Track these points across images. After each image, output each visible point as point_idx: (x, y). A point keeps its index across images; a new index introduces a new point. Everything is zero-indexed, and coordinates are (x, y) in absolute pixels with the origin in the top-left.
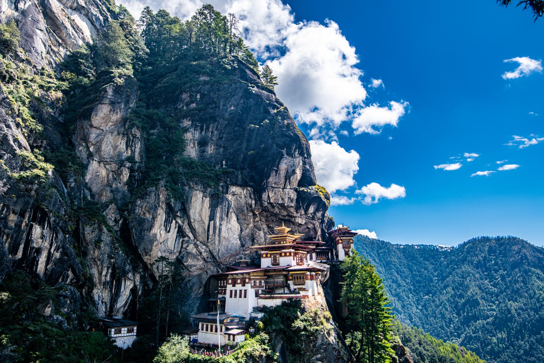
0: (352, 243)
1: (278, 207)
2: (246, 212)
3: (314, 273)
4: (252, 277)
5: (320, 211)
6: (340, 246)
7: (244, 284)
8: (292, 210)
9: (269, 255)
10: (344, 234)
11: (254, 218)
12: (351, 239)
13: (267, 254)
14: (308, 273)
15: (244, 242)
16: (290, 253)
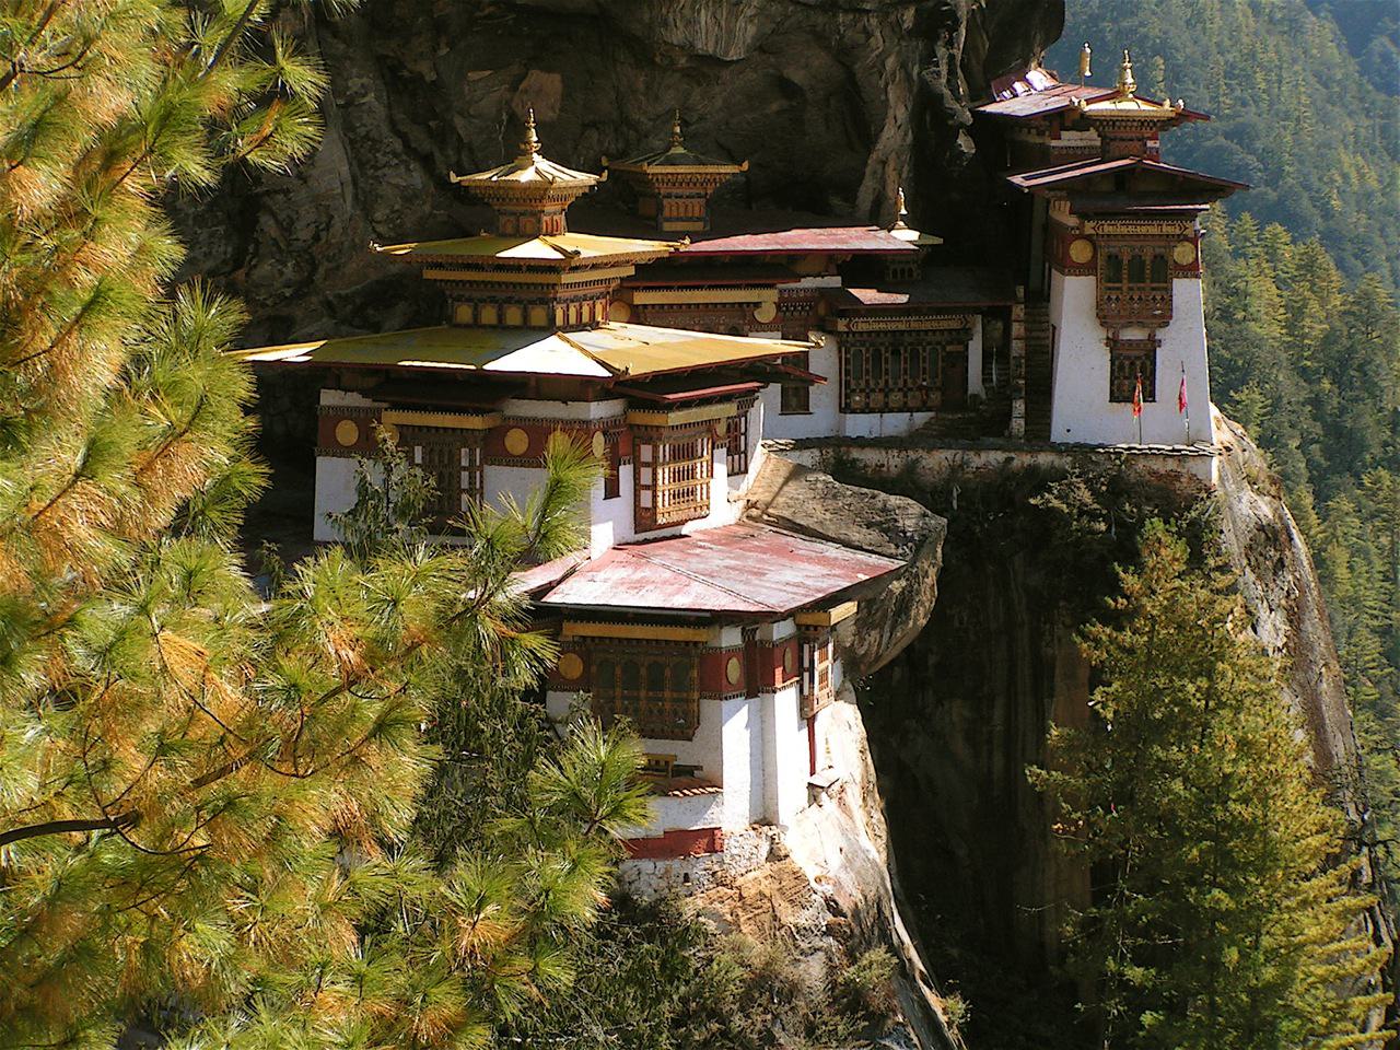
0: (1190, 271)
6: (1074, 296)
9: (386, 435)
14: (731, 638)
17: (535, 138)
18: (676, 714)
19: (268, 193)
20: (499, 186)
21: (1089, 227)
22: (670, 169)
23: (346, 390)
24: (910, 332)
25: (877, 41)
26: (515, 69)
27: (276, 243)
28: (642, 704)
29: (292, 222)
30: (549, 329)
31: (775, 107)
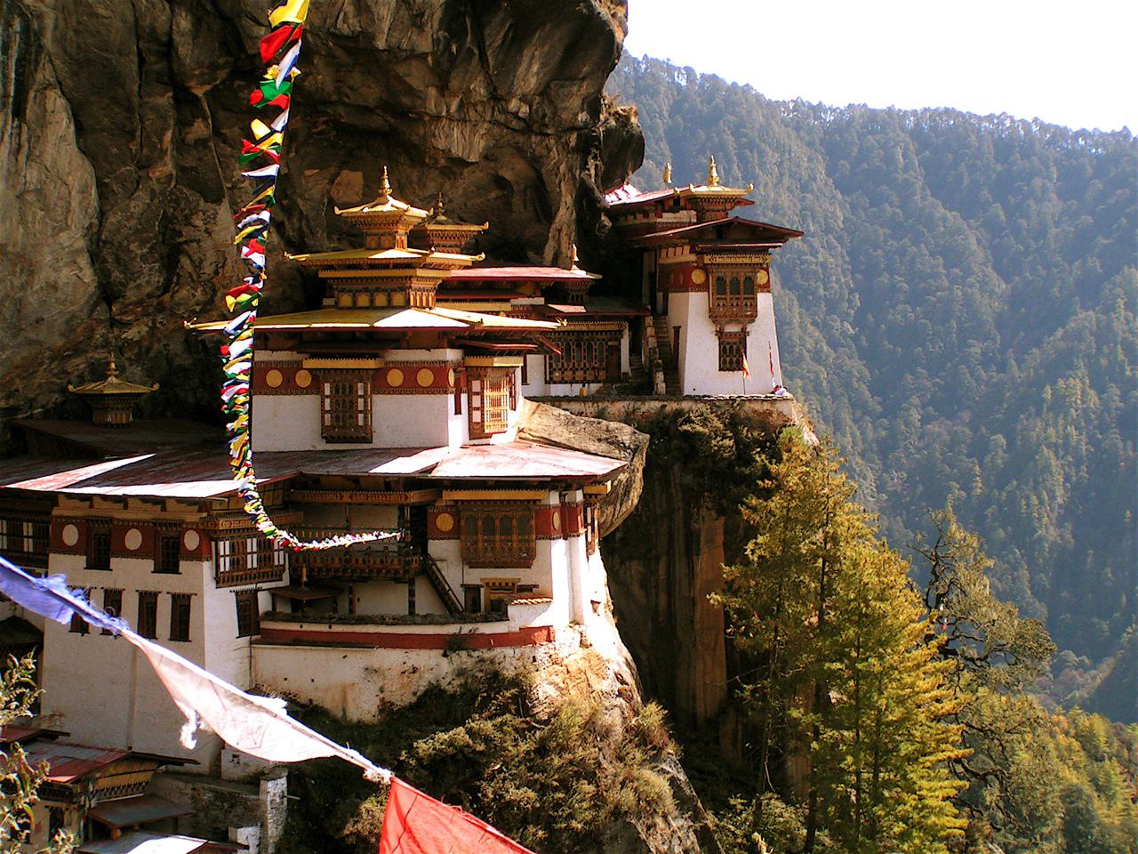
0: (766, 287)
1: (330, 55)
2: (136, 88)
3: (579, 496)
4: (223, 524)
5: (572, 79)
7: (168, 557)
8: (416, 76)
9: (303, 379)
10: (723, 231)
11: (183, 124)
12: (760, 266)
13: (290, 371)
14: (554, 499)
15: (117, 275)
16: (440, 369)
17: (387, 185)
18: (520, 549)
19: (186, 242)
20: (369, 215)
21: (707, 259)
22: (441, 227)
23: (273, 350)
24: (587, 332)
25: (554, 154)
26: (332, 170)
27: (191, 276)
28: (497, 545)
29: (201, 262)
30: (406, 306)
31: (493, 195)
